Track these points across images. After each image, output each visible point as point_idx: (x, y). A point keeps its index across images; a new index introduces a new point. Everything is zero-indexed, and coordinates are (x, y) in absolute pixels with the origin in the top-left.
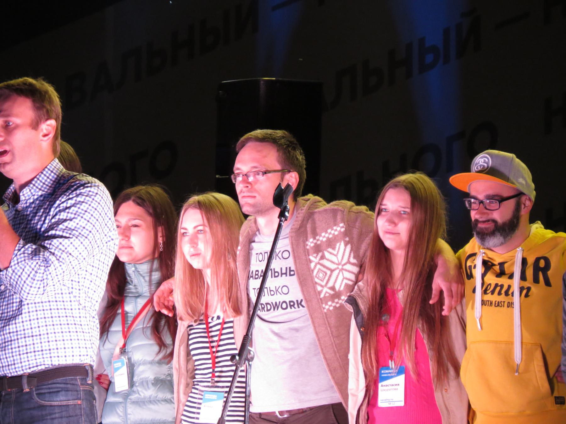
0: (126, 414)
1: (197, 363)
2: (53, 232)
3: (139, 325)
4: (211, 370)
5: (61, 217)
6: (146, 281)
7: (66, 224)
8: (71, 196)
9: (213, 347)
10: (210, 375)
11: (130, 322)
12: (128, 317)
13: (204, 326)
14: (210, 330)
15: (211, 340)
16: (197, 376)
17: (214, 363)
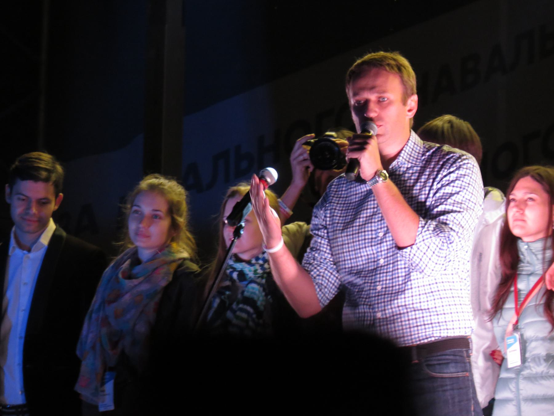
0: (518, 389)
3: (531, 302)
5: (446, 191)
6: (538, 259)
11: (522, 299)
12: (520, 294)
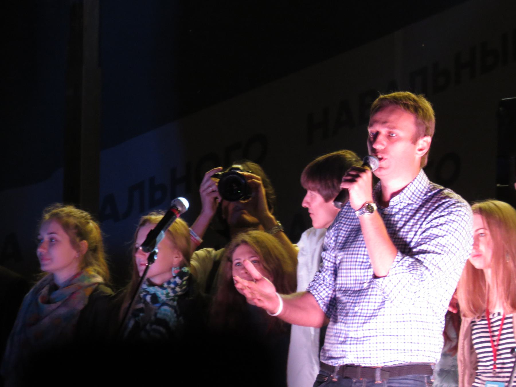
1: (479, 356)
2: (424, 247)
4: (492, 362)
7: (437, 240)
8: (443, 214)
9: (494, 341)
10: (492, 367)
13: (486, 322)
14: (491, 325)
15: (492, 334)
16: (479, 368)
17: (495, 356)
